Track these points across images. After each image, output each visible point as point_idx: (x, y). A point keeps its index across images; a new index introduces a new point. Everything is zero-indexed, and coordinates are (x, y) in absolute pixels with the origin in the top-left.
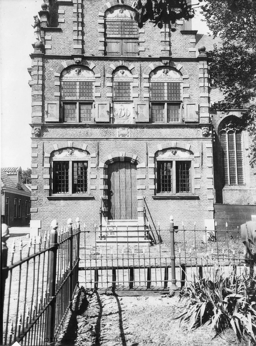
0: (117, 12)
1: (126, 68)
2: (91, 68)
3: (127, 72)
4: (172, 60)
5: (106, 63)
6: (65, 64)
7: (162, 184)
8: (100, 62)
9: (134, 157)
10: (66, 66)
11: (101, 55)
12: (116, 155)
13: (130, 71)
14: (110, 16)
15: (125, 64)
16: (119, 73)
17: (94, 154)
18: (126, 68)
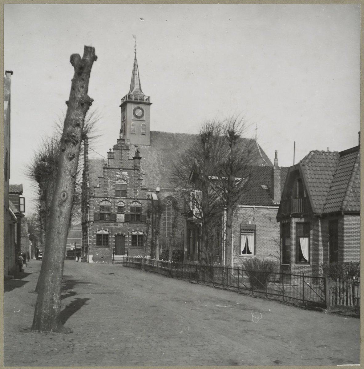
0: (119, 181)
1: (122, 202)
2: (110, 201)
3: (122, 203)
4: (138, 199)
5: (115, 200)
6: (101, 200)
7: (134, 244)
8: (113, 199)
9: (124, 234)
10: (101, 201)
11: (113, 197)
12: (118, 233)
13: (123, 203)
14: (117, 182)
15: (123, 200)
16: (119, 203)
17: (111, 233)
18: (122, 202)
